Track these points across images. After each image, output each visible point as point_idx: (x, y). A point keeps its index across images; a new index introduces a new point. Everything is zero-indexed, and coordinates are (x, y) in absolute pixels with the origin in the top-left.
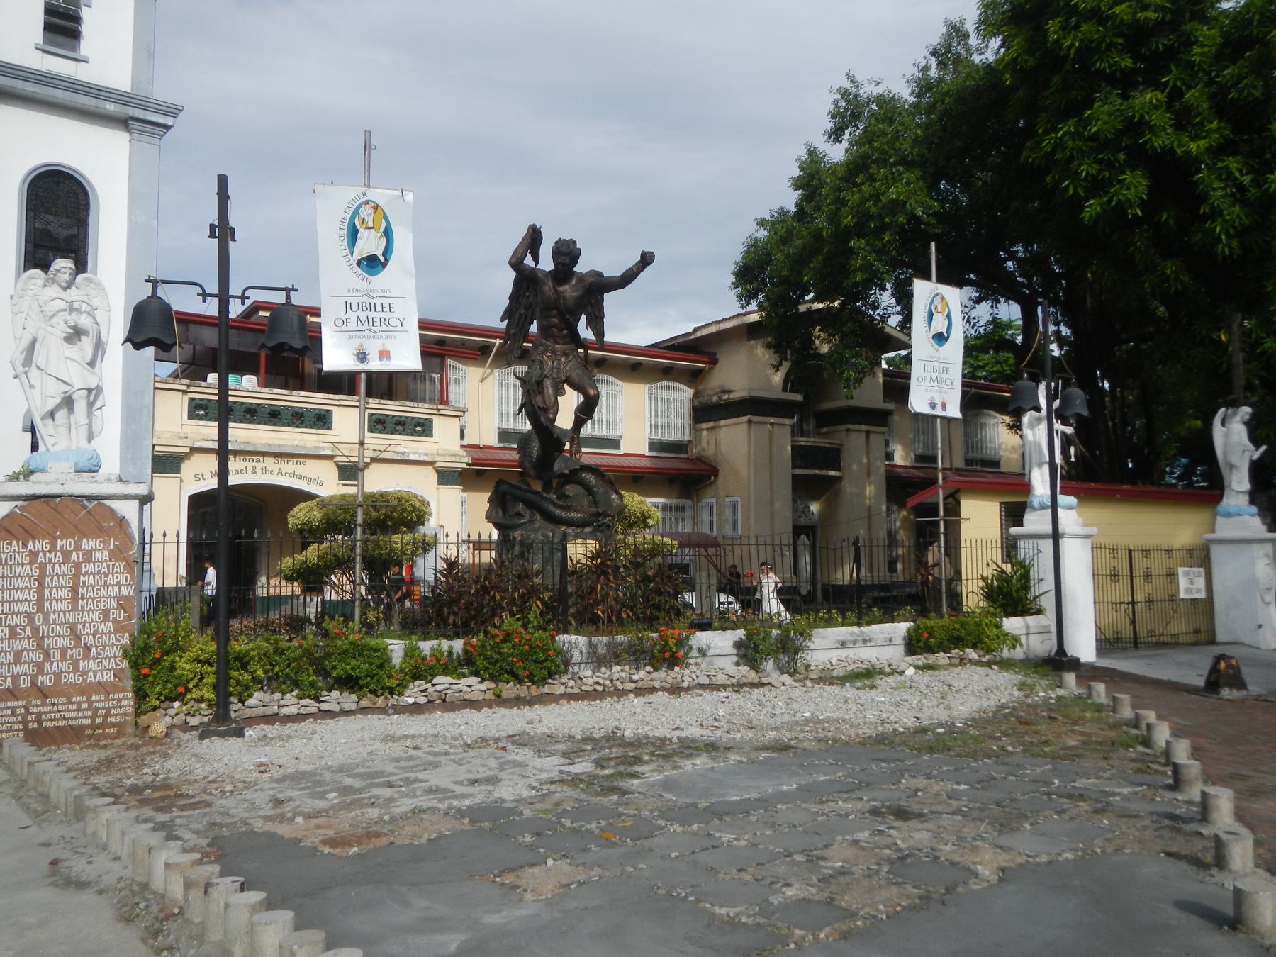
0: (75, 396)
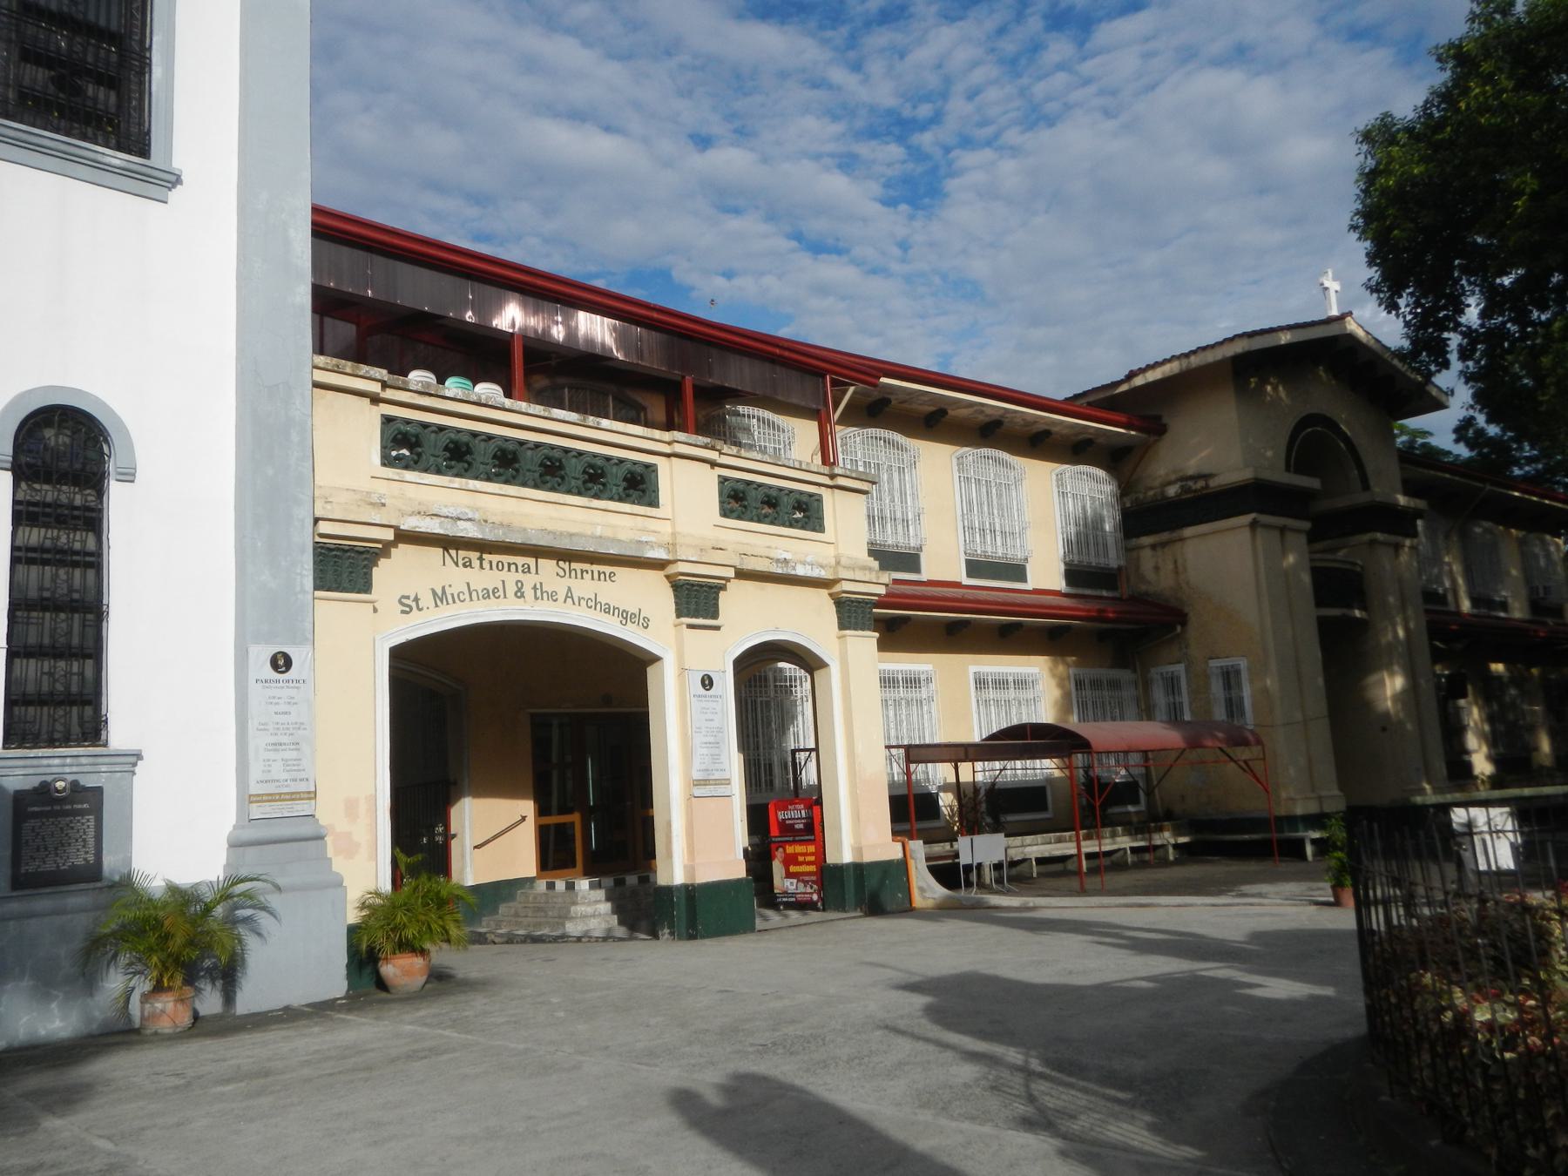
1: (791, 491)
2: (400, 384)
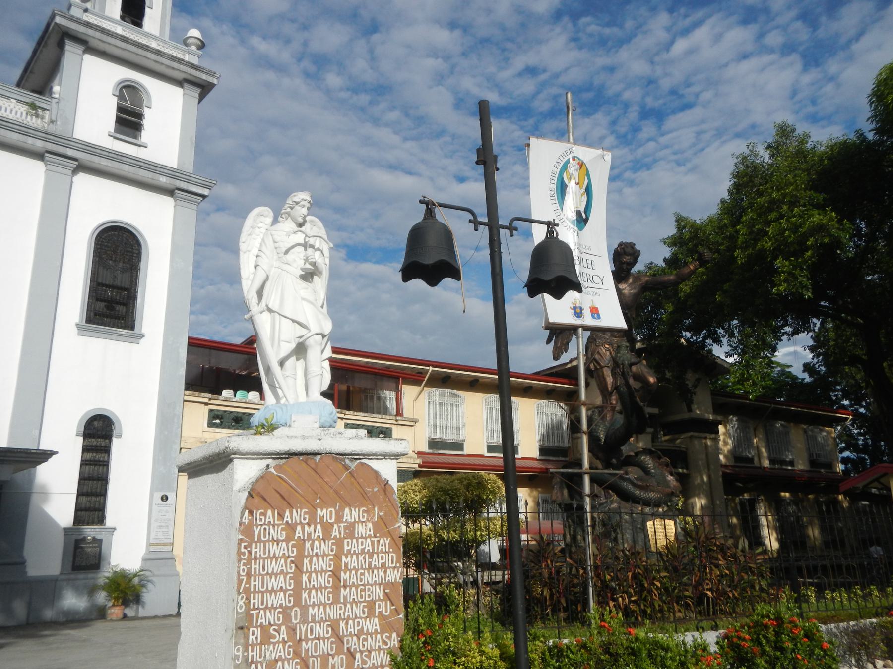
0: (308, 342)
1: (378, 427)
2: (216, 398)
